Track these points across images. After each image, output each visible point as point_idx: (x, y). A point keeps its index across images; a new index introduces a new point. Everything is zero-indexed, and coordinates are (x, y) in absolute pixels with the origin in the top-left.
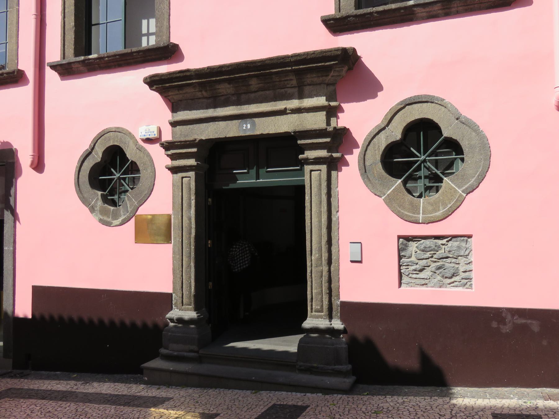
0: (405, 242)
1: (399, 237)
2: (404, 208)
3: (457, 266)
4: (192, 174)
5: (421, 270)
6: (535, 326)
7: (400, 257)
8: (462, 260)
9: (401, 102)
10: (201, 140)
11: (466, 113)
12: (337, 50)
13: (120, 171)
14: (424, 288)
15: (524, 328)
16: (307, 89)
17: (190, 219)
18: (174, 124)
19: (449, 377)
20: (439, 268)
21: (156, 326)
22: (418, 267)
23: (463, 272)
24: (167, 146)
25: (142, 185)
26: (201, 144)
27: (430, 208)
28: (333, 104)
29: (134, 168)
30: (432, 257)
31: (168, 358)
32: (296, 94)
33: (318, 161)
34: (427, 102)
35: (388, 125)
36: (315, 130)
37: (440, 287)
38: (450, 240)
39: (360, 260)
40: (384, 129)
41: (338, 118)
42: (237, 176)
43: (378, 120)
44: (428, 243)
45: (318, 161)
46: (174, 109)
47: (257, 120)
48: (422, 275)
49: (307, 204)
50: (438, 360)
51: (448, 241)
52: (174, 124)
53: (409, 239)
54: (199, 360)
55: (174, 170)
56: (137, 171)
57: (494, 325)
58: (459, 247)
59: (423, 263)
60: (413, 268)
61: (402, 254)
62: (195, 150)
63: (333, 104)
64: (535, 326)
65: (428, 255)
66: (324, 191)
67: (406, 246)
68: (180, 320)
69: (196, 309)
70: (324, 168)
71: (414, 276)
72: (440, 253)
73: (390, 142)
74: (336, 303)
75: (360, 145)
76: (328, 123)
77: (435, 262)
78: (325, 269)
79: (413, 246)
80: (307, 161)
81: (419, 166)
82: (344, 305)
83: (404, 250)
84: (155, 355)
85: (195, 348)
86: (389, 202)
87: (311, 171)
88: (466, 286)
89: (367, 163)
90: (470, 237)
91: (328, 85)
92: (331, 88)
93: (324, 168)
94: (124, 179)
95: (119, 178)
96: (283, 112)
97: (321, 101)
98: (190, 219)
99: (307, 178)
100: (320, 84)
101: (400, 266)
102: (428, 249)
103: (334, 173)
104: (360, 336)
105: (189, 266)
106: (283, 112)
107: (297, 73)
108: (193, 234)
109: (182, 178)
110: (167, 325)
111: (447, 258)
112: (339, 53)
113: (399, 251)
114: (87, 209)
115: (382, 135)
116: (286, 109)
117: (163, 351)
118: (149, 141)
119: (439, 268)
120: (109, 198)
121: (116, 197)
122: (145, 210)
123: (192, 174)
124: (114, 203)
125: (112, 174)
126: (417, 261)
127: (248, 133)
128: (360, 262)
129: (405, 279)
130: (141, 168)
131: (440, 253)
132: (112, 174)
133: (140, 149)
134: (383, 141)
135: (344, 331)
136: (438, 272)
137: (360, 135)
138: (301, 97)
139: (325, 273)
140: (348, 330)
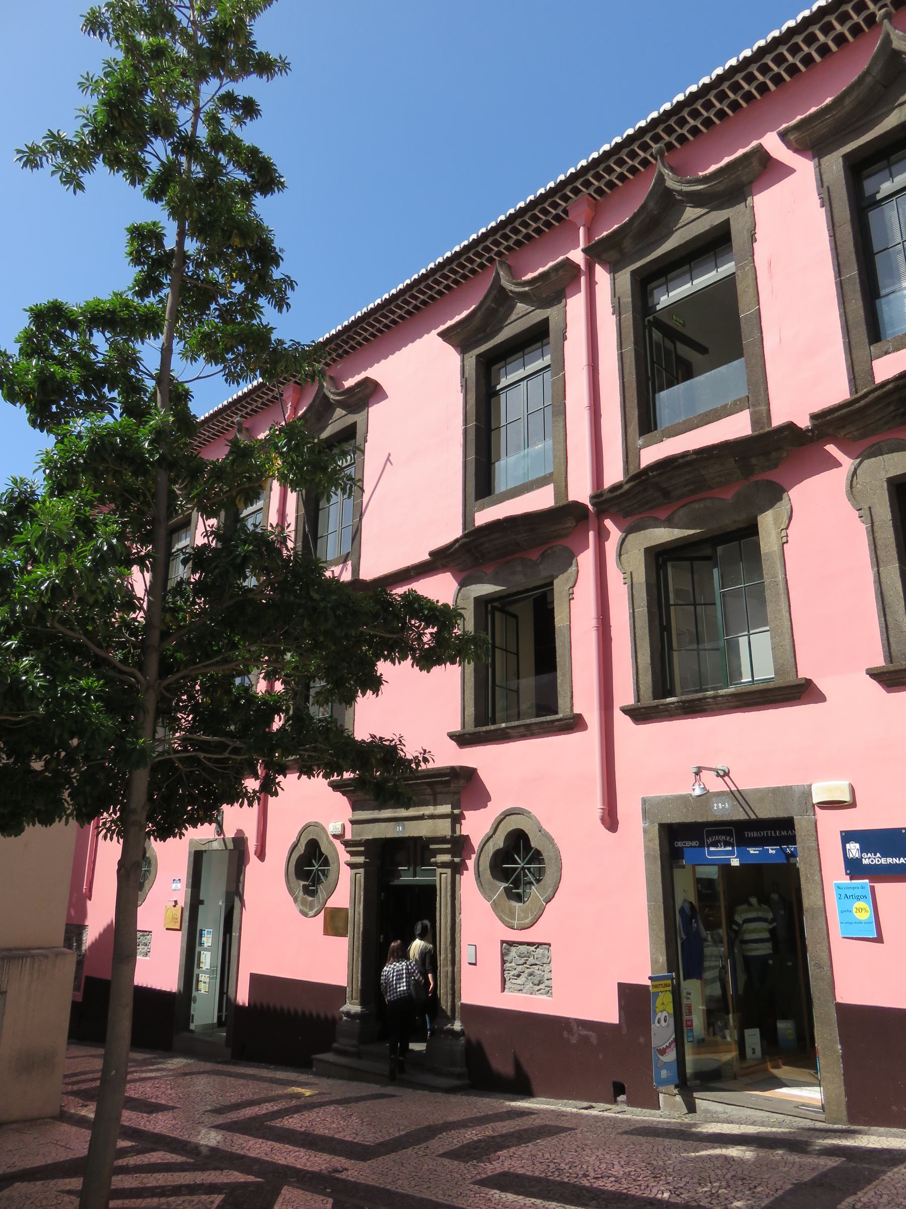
0: (508, 947)
1: (503, 942)
2: (505, 914)
3: (543, 973)
4: (362, 870)
5: (519, 976)
6: (593, 1037)
7: (504, 962)
8: (546, 968)
9: (501, 814)
10: (368, 840)
11: (546, 827)
12: (447, 768)
13: (524, 859)
14: (520, 994)
15: (585, 1039)
16: (439, 797)
17: (359, 914)
18: (353, 822)
19: (535, 1086)
20: (531, 974)
21: (334, 1018)
22: (515, 972)
23: (548, 980)
24: (347, 844)
25: (548, 878)
26: (368, 843)
27: (522, 915)
28: (456, 812)
29: (537, 857)
30: (525, 963)
31: (341, 1052)
32: (432, 801)
33: (444, 865)
34: (519, 814)
35: (494, 833)
36: (438, 837)
37: (531, 994)
38: (538, 947)
39: (474, 962)
40: (491, 837)
41: (461, 825)
42: (402, 872)
43: (487, 829)
44: (523, 949)
45: (444, 865)
46: (354, 808)
47: (406, 823)
48: (519, 981)
49: (438, 905)
50: (530, 1070)
51: (536, 948)
52: (353, 822)
53: (511, 944)
54: (359, 1055)
55: (352, 866)
56: (541, 861)
57: (565, 1034)
58: (543, 955)
59: (520, 968)
60: (512, 973)
61: (505, 959)
62: (362, 849)
63: (456, 812)
64: (593, 1037)
65: (523, 961)
66: (449, 894)
67: (509, 950)
68: (348, 1014)
69: (363, 1003)
70: (449, 871)
71: (514, 981)
72: (531, 960)
73: (496, 849)
74: (458, 1004)
75: (476, 849)
76: (453, 830)
77: (528, 968)
78: (450, 969)
79: (514, 951)
80: (435, 864)
81: (518, 876)
82: (464, 1006)
83: (507, 954)
84: (327, 1049)
85: (355, 1042)
86: (495, 906)
87: (441, 874)
88: (549, 994)
89: (481, 869)
90: (549, 945)
91: (454, 793)
92: (456, 797)
93: (449, 871)
94: (529, 869)
95: (523, 869)
96: (421, 818)
97: (446, 809)
98: (359, 914)
99: (438, 879)
100: (447, 793)
101: (503, 971)
102: (523, 955)
103: (458, 876)
104: (473, 1038)
105: (357, 960)
106: (421, 818)
107: (429, 784)
108: (361, 929)
109: (356, 874)
110: (341, 1018)
111: (536, 965)
112: (449, 771)
113: (503, 955)
114: (488, 905)
115: (490, 843)
116: (423, 815)
117: (335, 1045)
118: (335, 836)
119: (531, 974)
120: (514, 891)
121: (520, 891)
122: (332, 903)
123: (362, 870)
124: (519, 898)
125: (516, 862)
126: (516, 966)
127: (401, 835)
128: (475, 964)
129: (508, 985)
130: (330, 862)
131: (531, 960)
132: (516, 862)
133: (331, 843)
134: (491, 849)
135: (462, 1033)
136: (529, 978)
137: (476, 843)
138: (435, 804)
139: (450, 974)
140: (466, 1032)
